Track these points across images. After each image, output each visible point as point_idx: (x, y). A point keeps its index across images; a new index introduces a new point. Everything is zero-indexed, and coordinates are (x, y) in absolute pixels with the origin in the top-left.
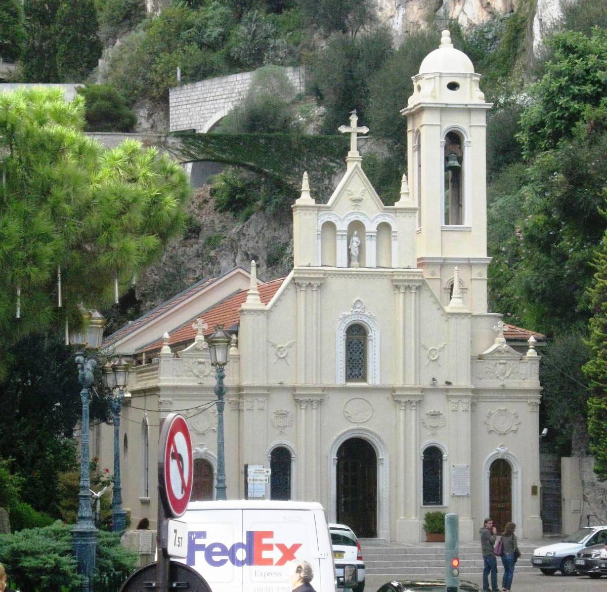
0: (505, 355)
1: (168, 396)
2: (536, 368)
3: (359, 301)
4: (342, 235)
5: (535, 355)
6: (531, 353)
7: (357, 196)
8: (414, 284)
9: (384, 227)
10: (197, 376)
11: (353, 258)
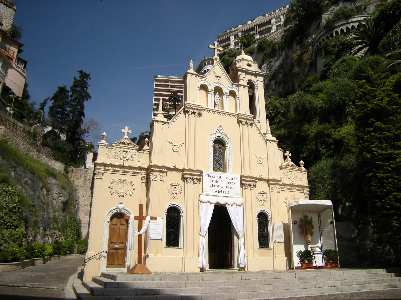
0: (291, 167)
1: (102, 169)
3: (220, 126)
4: (211, 92)
5: (304, 169)
6: (303, 168)
8: (249, 121)
10: (121, 159)
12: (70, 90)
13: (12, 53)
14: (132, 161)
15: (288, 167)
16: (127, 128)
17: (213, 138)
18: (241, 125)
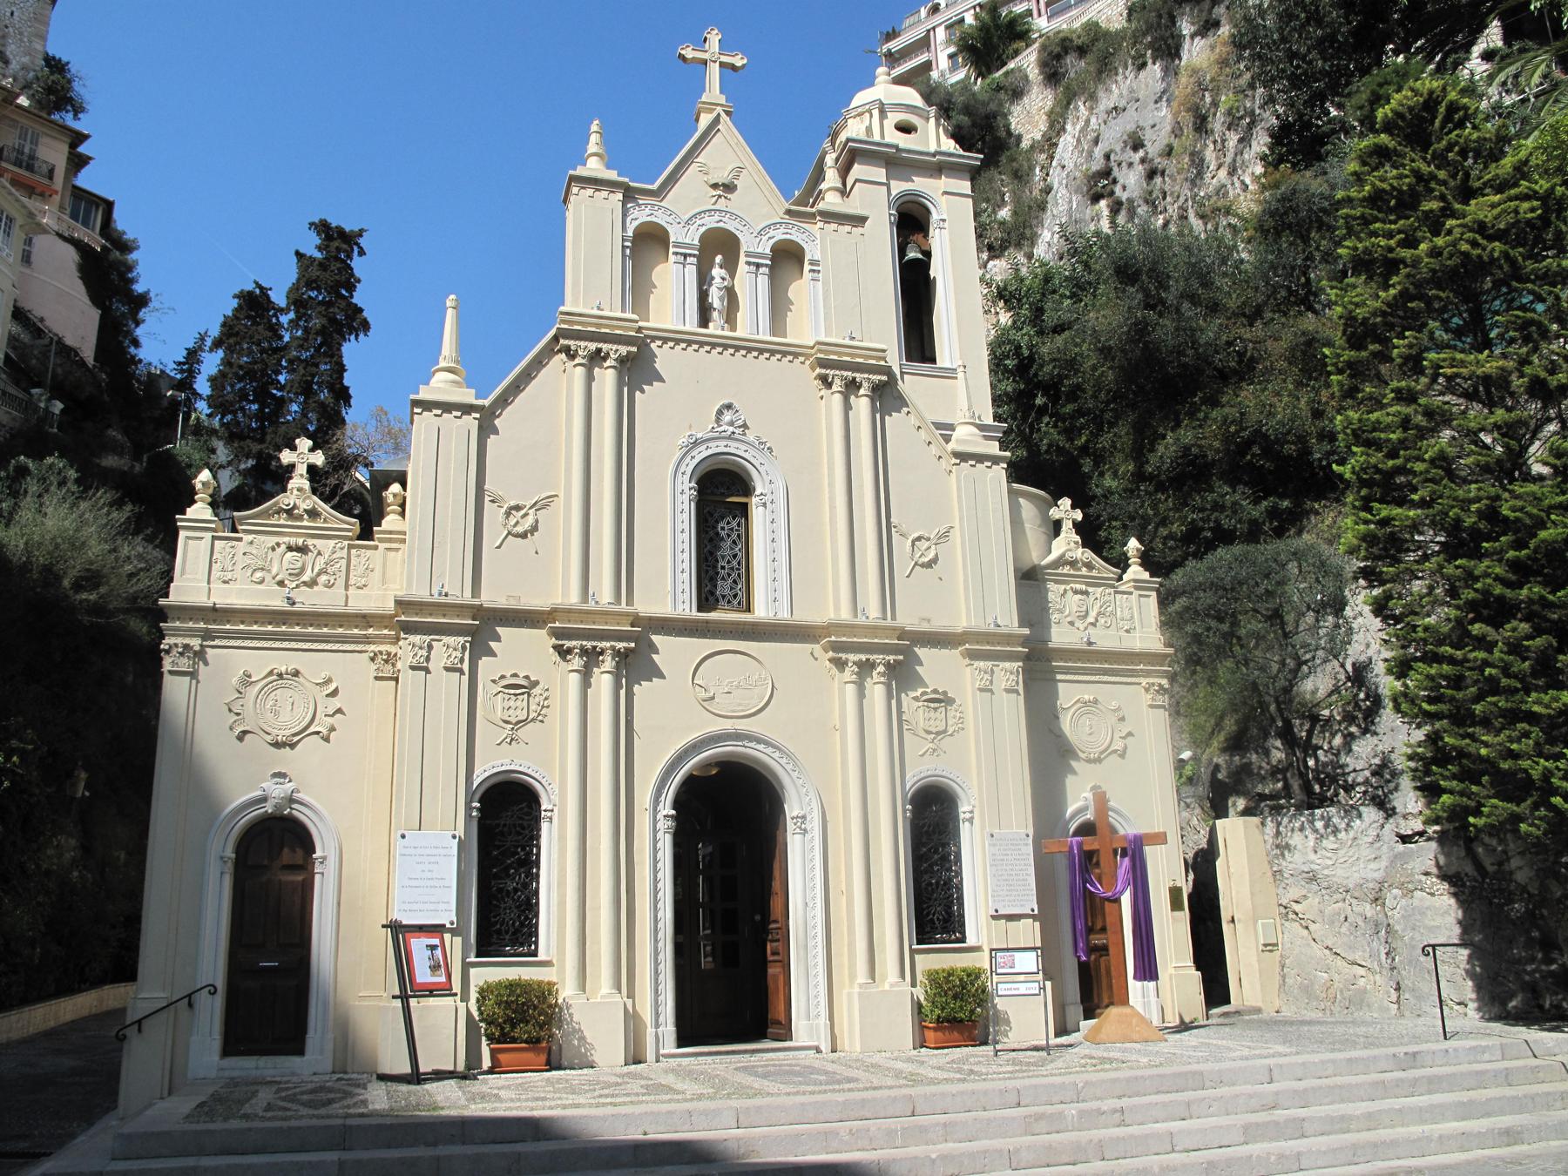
1: (191, 633)
2: (1152, 601)
3: (729, 407)
4: (685, 256)
5: (1146, 575)
6: (1135, 571)
7: (722, 176)
12: (282, 303)
13: (45, 169)
15: (1066, 570)
16: (304, 444)
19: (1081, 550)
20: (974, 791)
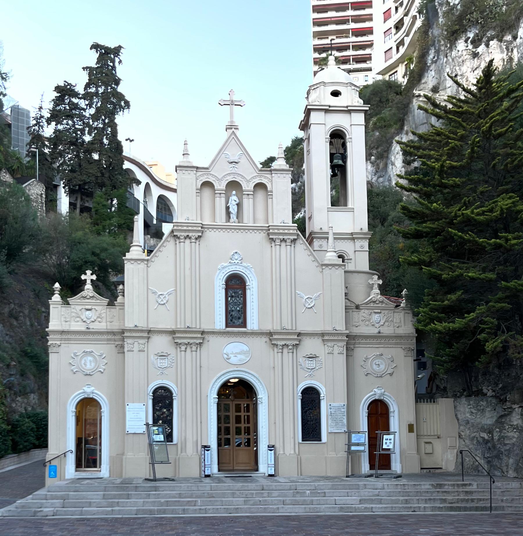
0: (380, 305)
3: (236, 253)
8: (289, 237)
9: (260, 186)
10: (84, 322)
11: (231, 216)
14: (100, 322)
15: (372, 305)
16: (89, 272)
17: (223, 275)
18: (273, 245)
19: (379, 296)
20: (324, 390)
